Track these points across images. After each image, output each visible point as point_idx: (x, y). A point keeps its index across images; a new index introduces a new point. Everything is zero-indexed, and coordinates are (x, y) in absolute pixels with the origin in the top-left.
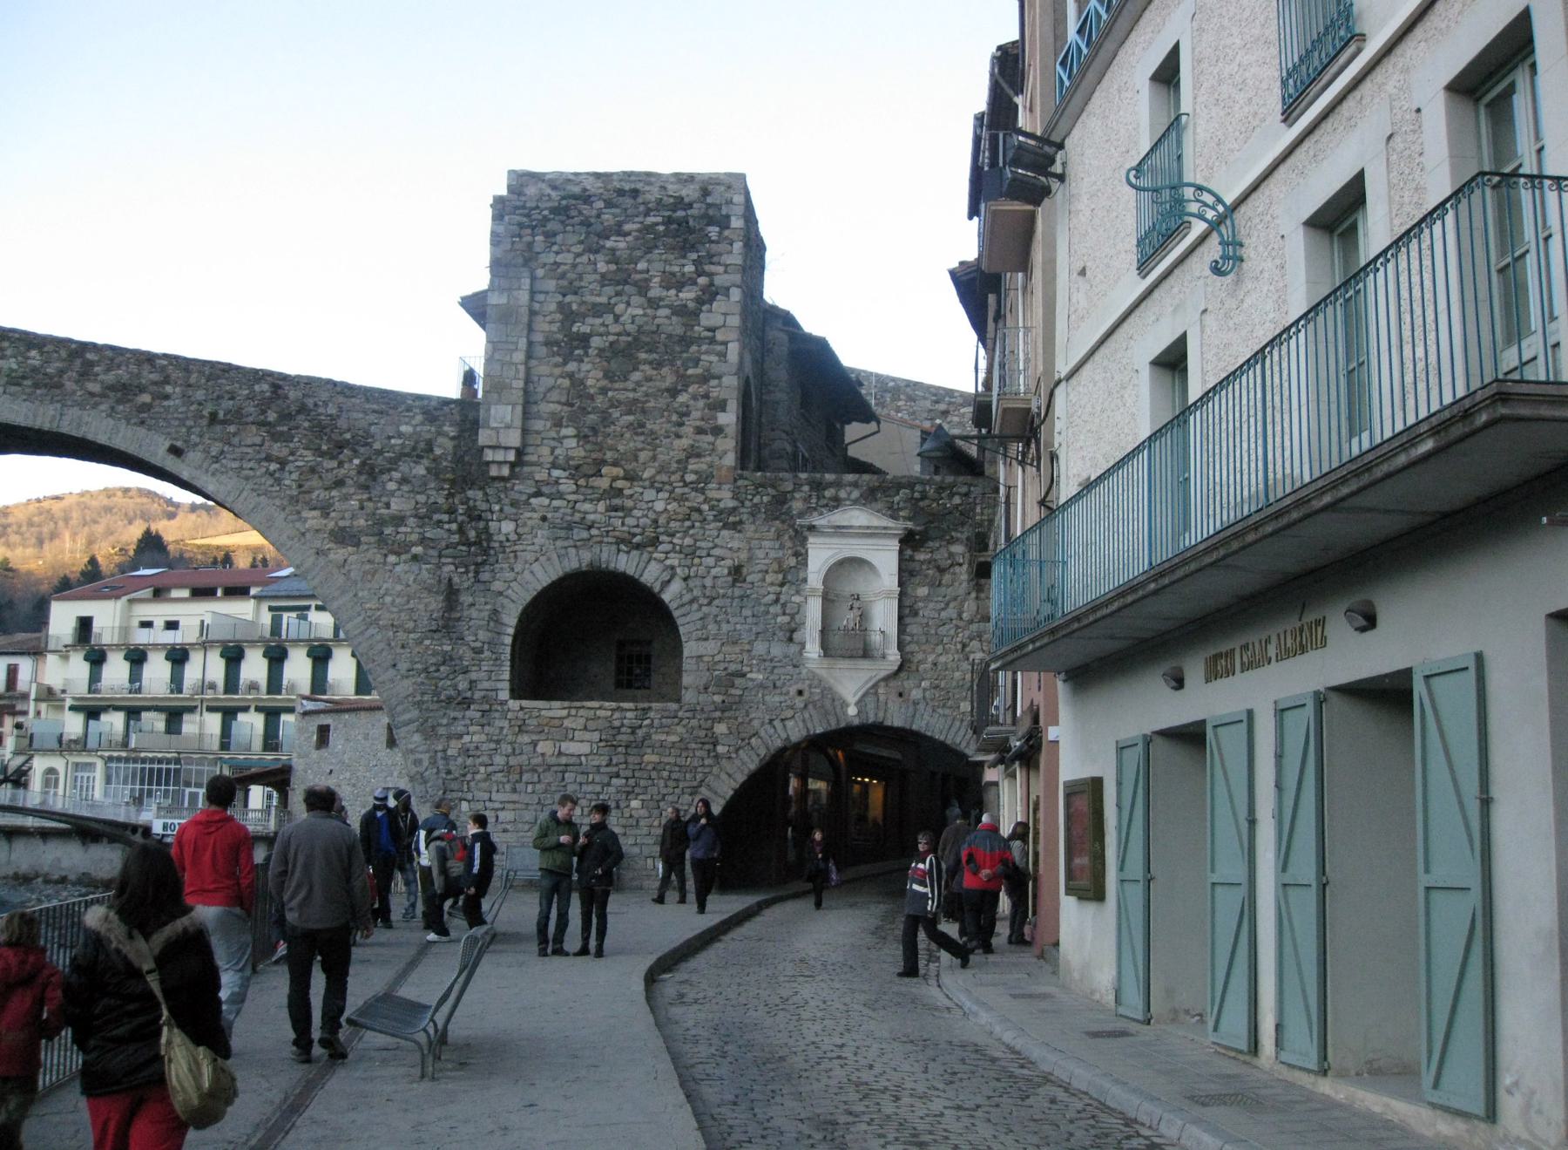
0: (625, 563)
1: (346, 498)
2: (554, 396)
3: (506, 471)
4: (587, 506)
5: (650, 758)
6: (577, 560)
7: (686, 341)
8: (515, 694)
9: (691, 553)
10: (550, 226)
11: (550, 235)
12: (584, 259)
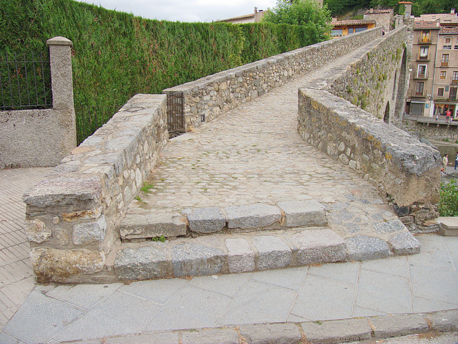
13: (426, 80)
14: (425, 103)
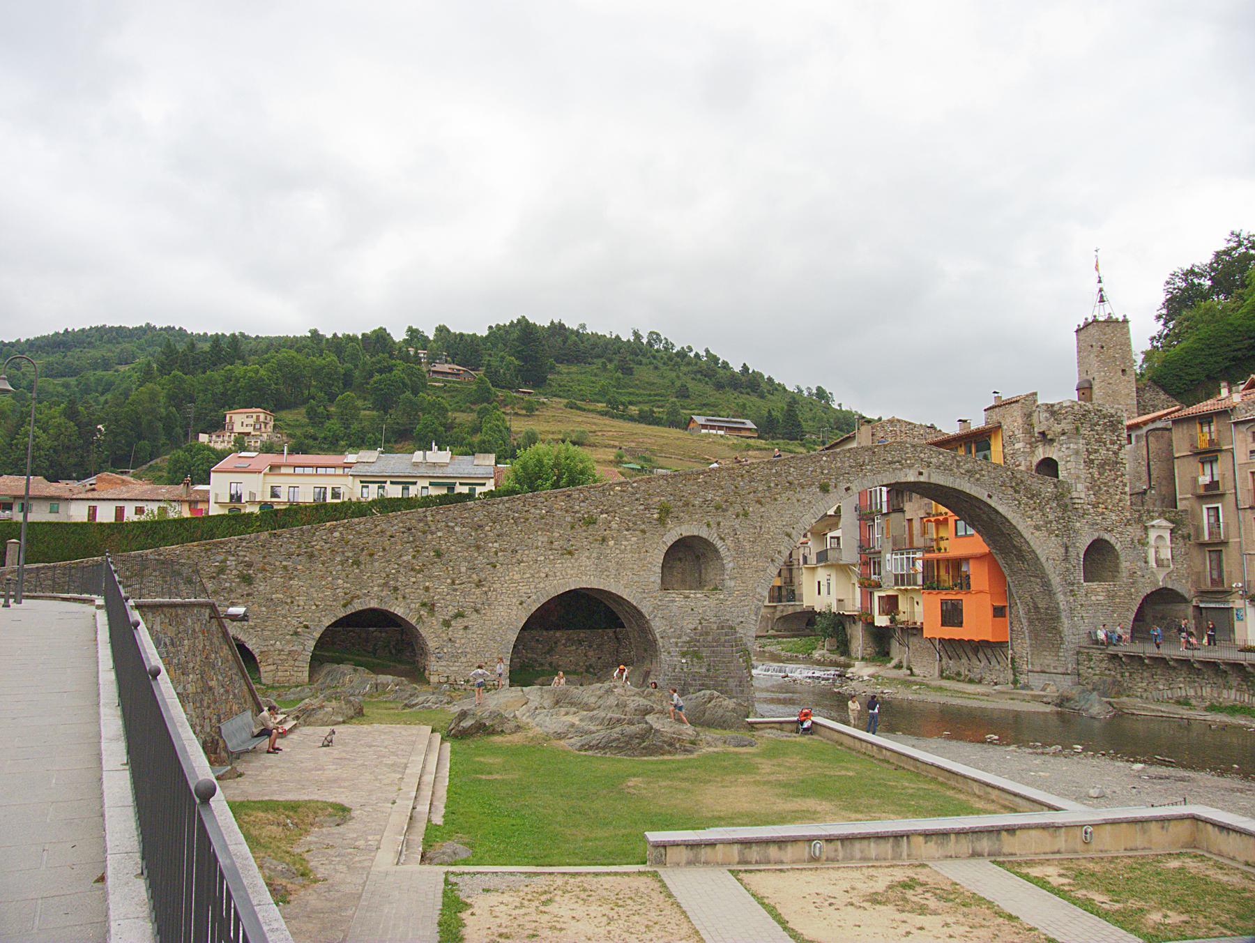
0: (1107, 537)
1: (1037, 514)
2: (1088, 480)
4: (1096, 518)
5: (1117, 600)
6: (1096, 536)
7: (1117, 463)
9: (1121, 533)
10: (1082, 421)
11: (1082, 424)
12: (1091, 433)
13: (1225, 543)
14: (1230, 606)
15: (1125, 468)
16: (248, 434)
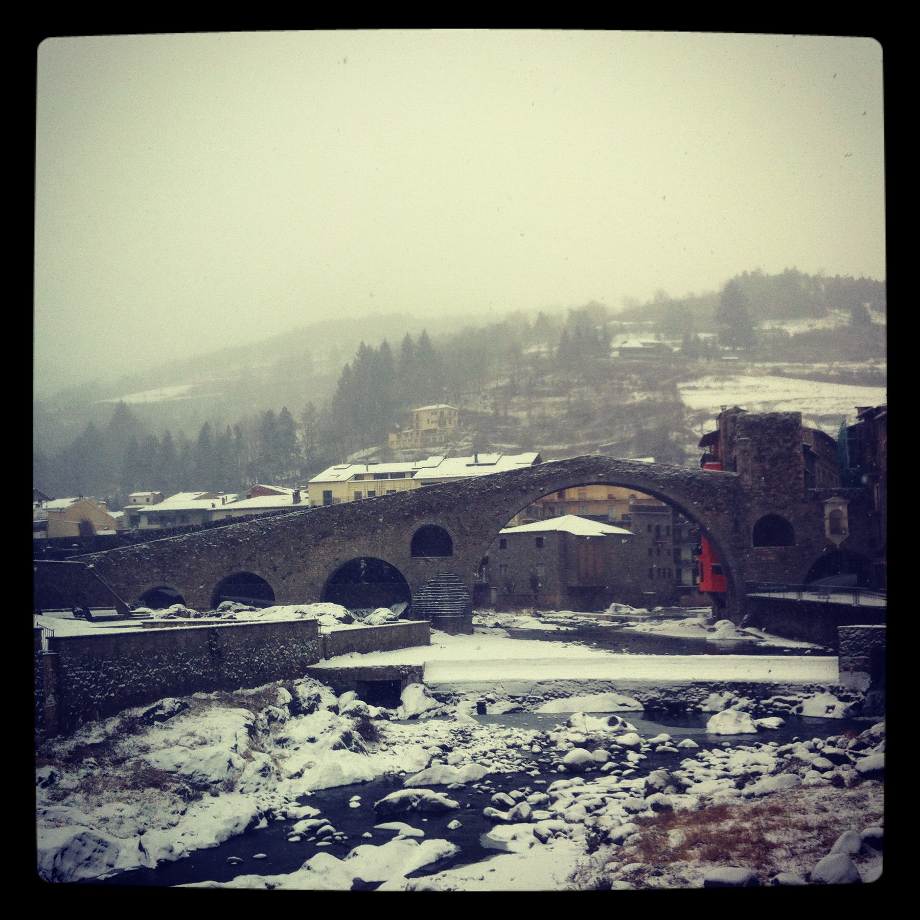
0: (779, 513)
3: (748, 491)
8: (755, 546)
15: (800, 460)
16: (435, 430)
